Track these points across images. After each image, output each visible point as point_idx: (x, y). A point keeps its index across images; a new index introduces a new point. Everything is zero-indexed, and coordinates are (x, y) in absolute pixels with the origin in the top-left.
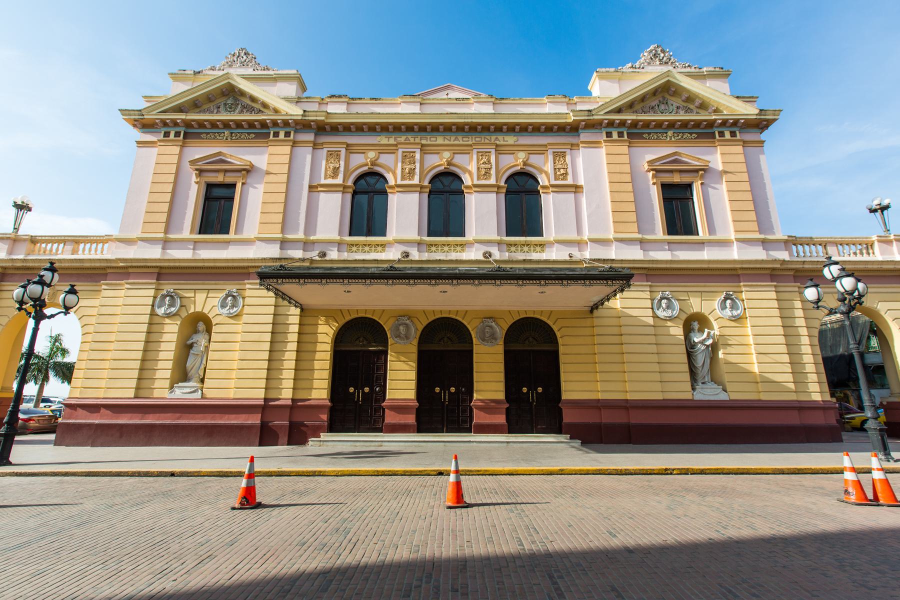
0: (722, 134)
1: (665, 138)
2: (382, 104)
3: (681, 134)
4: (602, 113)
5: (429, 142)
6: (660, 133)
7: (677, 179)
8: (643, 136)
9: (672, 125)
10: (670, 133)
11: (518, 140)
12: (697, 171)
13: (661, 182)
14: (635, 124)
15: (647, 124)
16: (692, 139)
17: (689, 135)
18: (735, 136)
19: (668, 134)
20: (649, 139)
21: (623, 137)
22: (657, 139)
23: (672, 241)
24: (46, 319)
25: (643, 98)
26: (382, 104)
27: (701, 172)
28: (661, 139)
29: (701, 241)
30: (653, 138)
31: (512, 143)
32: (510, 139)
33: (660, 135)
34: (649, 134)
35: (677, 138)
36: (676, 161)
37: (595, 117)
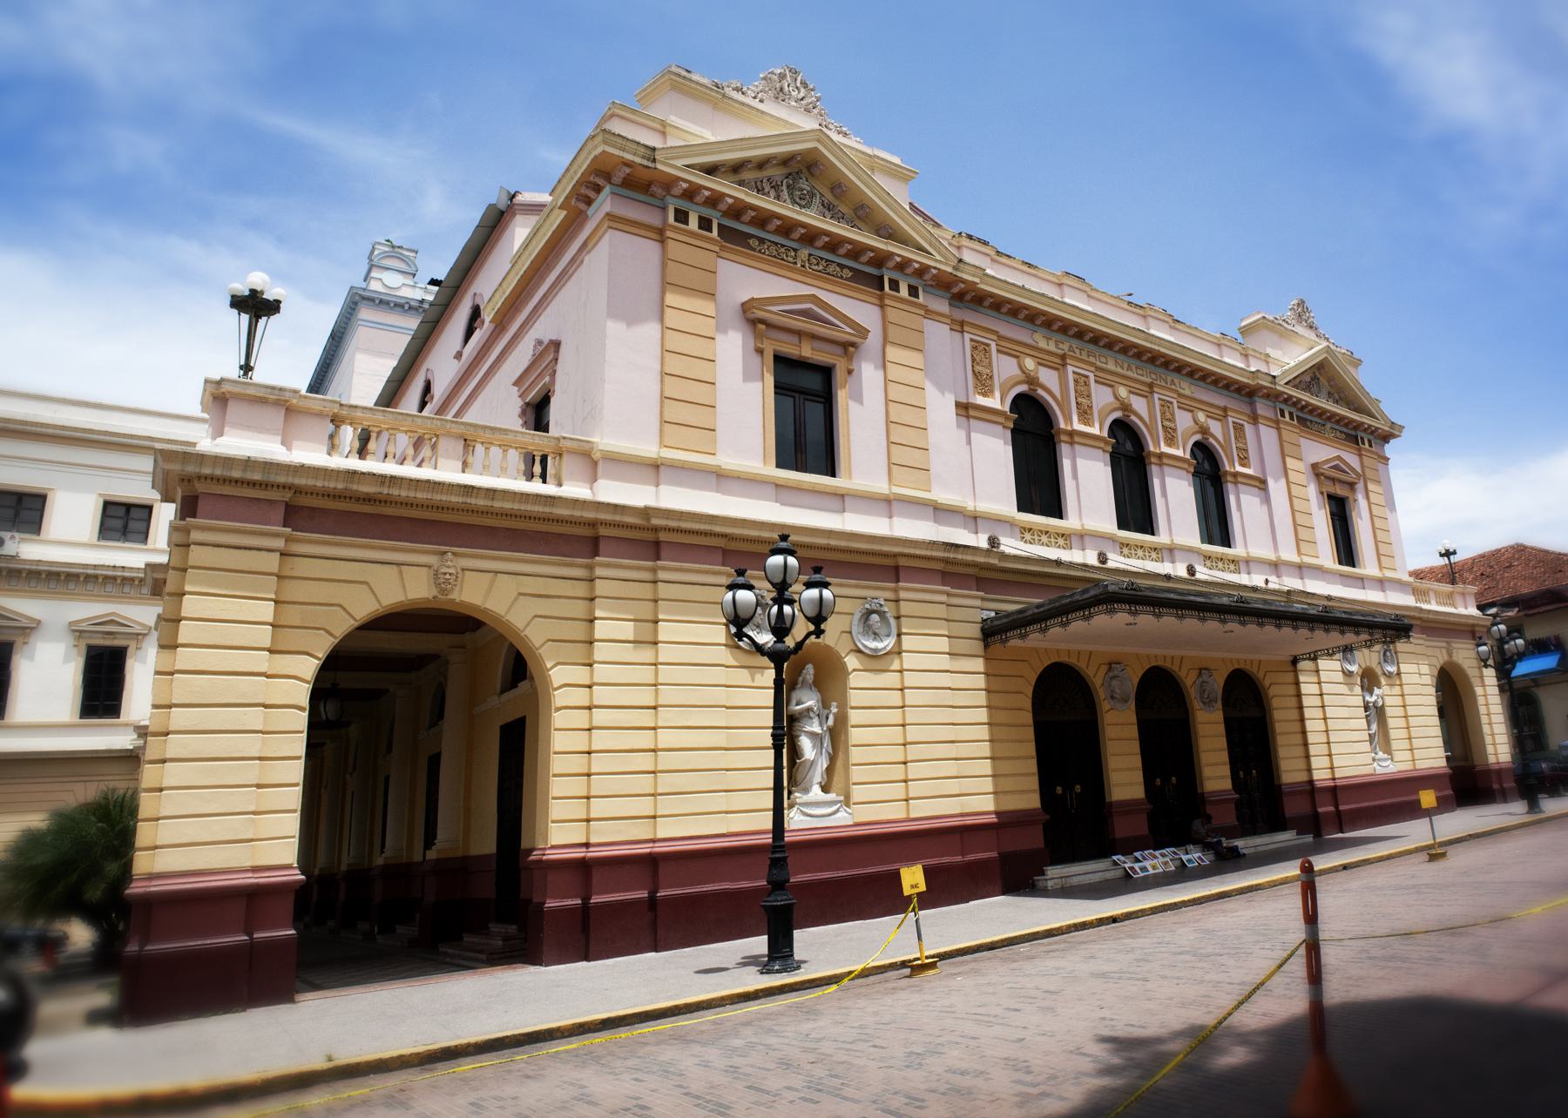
0: (895, 285)
1: (791, 259)
3: (823, 262)
6: (783, 246)
7: (807, 351)
8: (749, 244)
9: (811, 237)
10: (804, 253)
13: (774, 351)
14: (738, 210)
15: (762, 219)
16: (842, 277)
17: (838, 269)
18: (917, 297)
19: (799, 253)
20: (760, 251)
21: (710, 230)
22: (775, 257)
25: (762, 164)
28: (783, 259)
30: (767, 253)
33: (783, 250)
34: (762, 241)
35: (816, 267)
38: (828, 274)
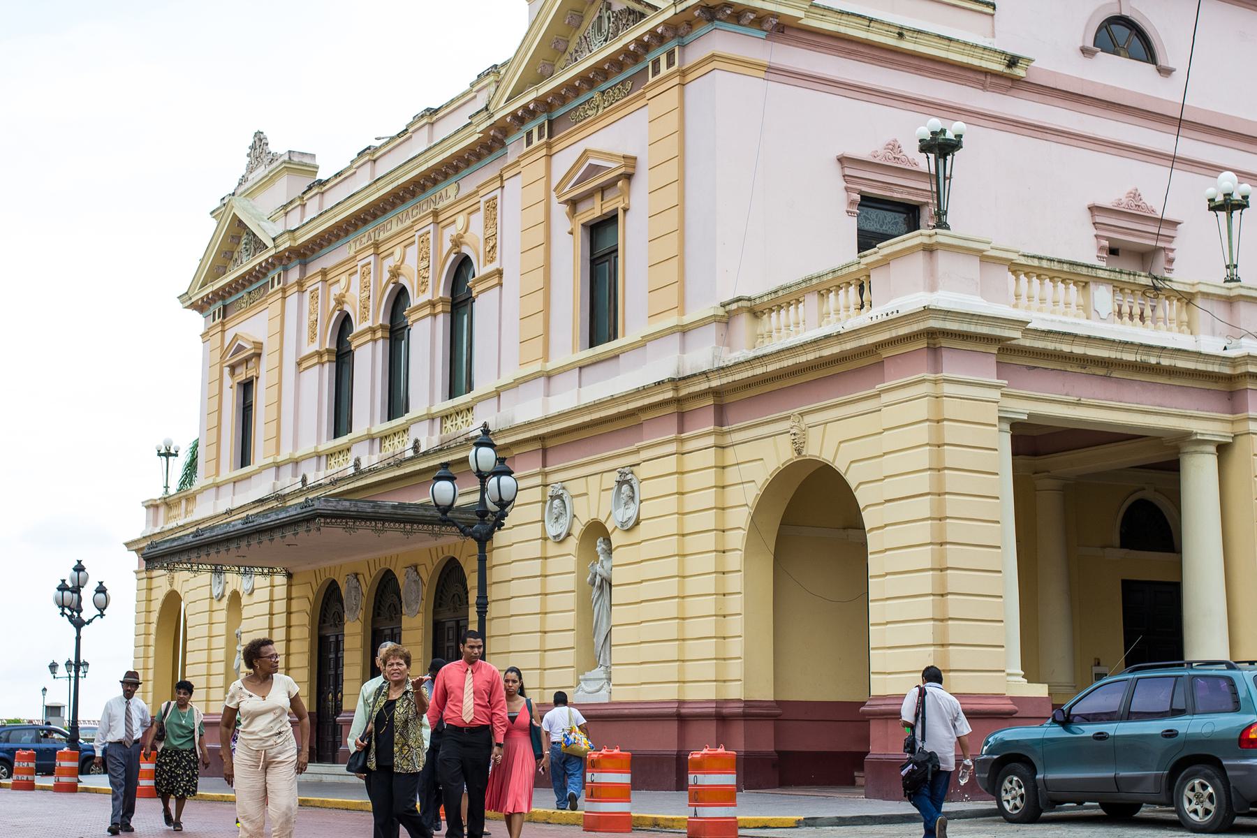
2: (346, 178)
4: (502, 104)
5: (388, 234)
10: (595, 94)
11: (459, 185)
12: (612, 184)
14: (544, 104)
23: (581, 364)
24: (75, 629)
26: (346, 178)
27: (620, 183)
29: (612, 354)
31: (452, 200)
32: (449, 192)
34: (576, 109)
36: (594, 170)
37: (496, 117)
38: (617, 100)
